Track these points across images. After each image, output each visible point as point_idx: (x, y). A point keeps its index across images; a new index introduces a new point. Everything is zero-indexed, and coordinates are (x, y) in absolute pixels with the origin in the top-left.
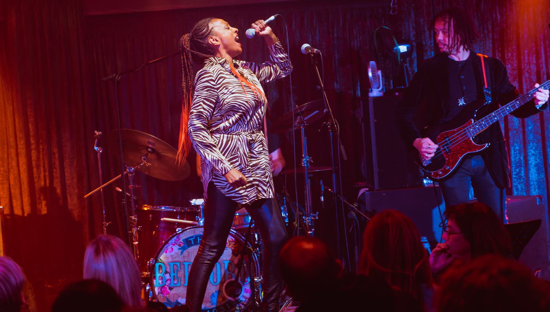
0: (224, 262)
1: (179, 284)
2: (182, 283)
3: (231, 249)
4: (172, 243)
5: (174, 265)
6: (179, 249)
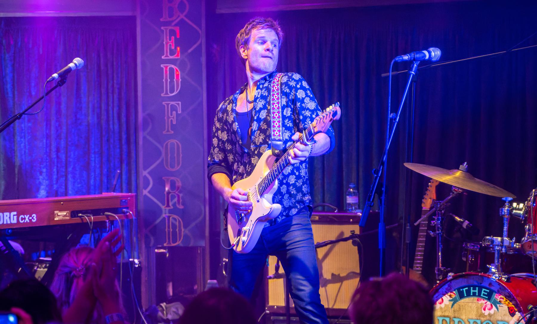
3: (507, 307)
4: (443, 292)
5: (443, 320)
6: (450, 301)
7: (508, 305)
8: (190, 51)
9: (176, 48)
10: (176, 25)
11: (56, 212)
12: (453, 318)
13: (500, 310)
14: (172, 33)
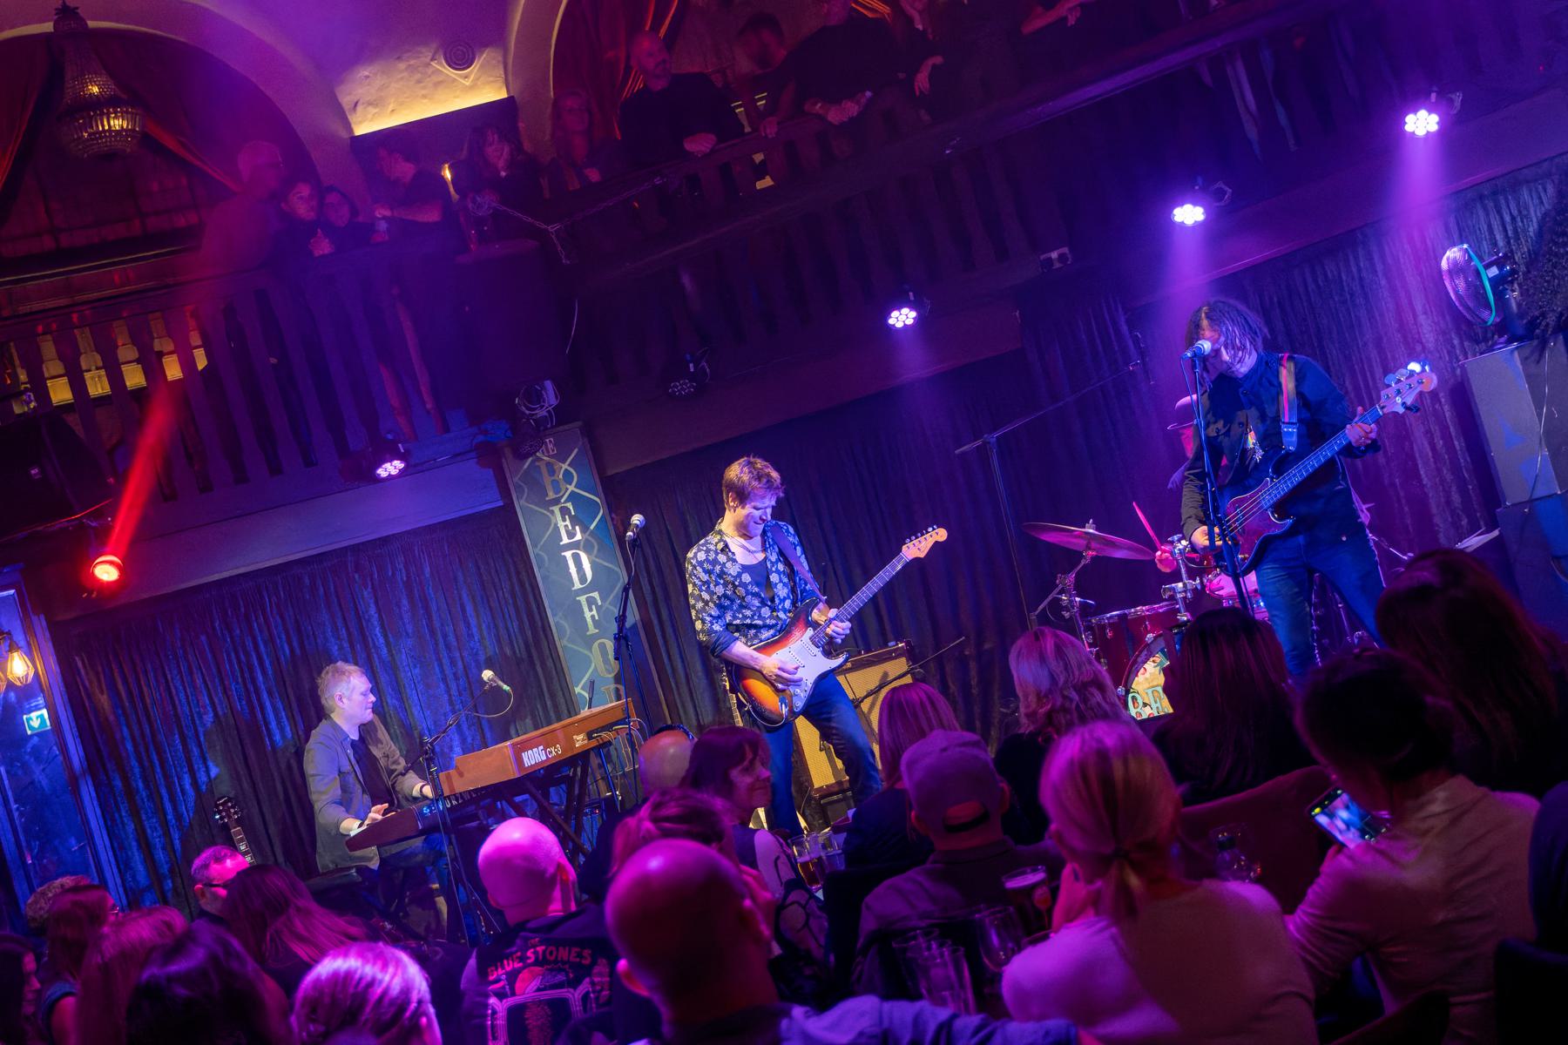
8: (592, 527)
9: (574, 528)
10: (565, 502)
11: (575, 737)
14: (564, 511)
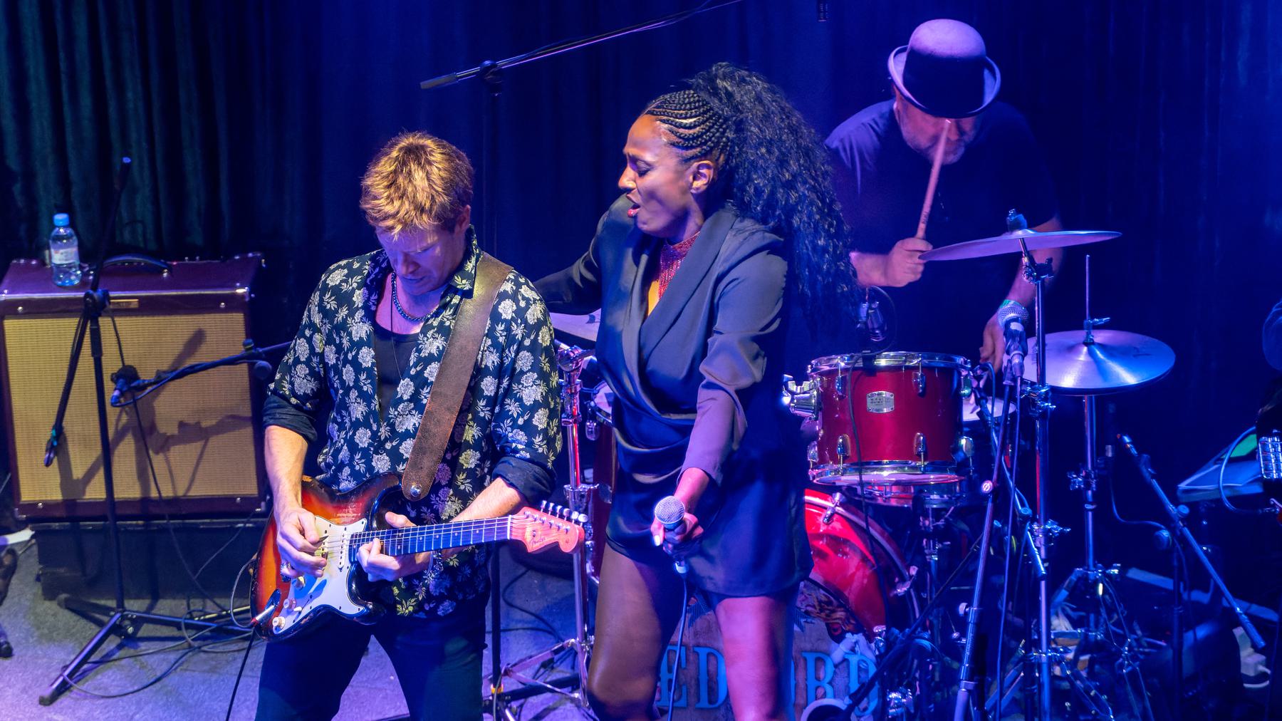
0: (805, 654)
1: (682, 703)
2: (693, 700)
7: (825, 620)
12: (694, 646)
13: (807, 631)
